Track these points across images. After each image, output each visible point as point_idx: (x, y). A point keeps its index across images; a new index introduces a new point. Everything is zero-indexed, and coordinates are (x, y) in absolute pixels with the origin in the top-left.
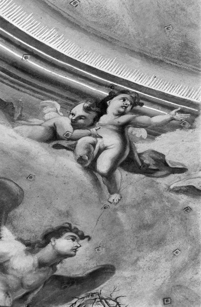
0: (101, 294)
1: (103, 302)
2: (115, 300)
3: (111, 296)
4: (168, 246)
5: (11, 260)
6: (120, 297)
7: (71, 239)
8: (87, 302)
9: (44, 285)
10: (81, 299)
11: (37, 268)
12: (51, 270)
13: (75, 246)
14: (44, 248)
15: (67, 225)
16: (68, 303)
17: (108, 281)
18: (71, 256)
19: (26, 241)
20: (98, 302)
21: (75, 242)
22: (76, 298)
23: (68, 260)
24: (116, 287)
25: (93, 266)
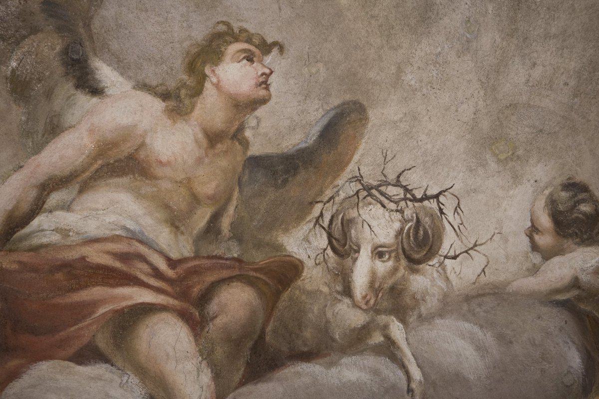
0: (362, 177)
1: (375, 196)
2: (397, 184)
3: (385, 176)
4: (446, 20)
5: (148, 141)
6: (403, 172)
7: (244, 58)
8: (344, 205)
9: (240, 188)
10: (328, 202)
11: (207, 148)
13: (260, 73)
14: (201, 97)
15: (222, 28)
16: (308, 220)
17: (363, 141)
18: (264, 101)
19: (157, 86)
20: (365, 198)
21: (255, 64)
22: (317, 202)
23: (261, 112)
24: (384, 151)
25: (320, 116)
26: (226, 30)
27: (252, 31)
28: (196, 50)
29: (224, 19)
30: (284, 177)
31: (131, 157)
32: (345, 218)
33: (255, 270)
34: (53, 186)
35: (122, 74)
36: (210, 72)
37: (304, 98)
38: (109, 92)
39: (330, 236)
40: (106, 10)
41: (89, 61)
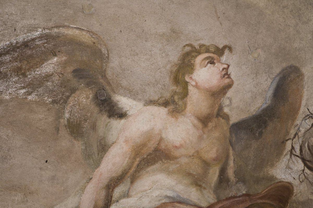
5: (164, 136)
7: (208, 63)
8: (306, 136)
9: (232, 147)
10: (294, 138)
11: (203, 128)
12: (222, 121)
13: (221, 69)
14: (188, 97)
15: (188, 49)
16: (284, 154)
17: (305, 90)
18: (229, 86)
19: (159, 99)
21: (216, 65)
22: (287, 140)
23: (230, 93)
25: (269, 83)
26: (191, 49)
27: (207, 44)
28: (176, 68)
29: (188, 43)
30: (259, 130)
31: (157, 150)
32: (310, 145)
33: (261, 198)
34: (114, 185)
35: (134, 99)
36: (189, 79)
37: (255, 75)
38: (129, 113)
39: (304, 160)
40: (112, 62)
41: (112, 98)
